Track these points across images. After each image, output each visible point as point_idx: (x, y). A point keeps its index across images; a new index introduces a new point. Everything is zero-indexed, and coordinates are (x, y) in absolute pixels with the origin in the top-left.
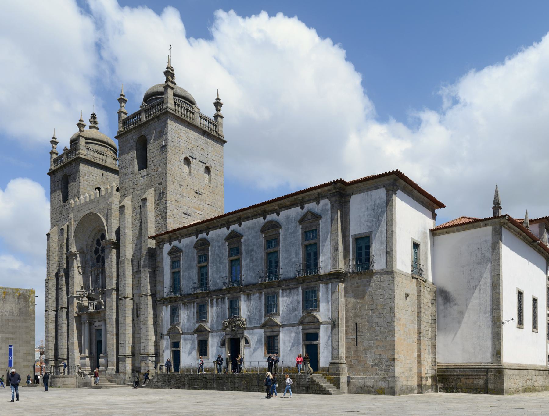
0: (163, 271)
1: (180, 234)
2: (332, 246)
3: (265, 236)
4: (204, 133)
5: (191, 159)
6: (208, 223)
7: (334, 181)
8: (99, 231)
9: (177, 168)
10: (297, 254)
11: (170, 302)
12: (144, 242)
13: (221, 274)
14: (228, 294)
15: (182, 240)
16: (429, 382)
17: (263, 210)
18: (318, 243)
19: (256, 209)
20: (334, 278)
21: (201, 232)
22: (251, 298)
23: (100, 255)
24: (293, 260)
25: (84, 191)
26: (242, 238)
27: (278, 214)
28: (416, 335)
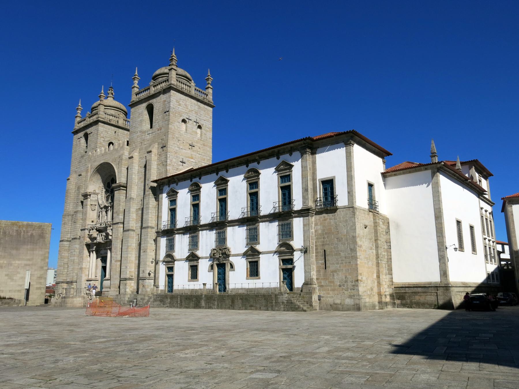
1: (178, 179)
2: (303, 188)
4: (198, 100)
5: (187, 120)
6: (201, 170)
7: (303, 138)
9: (176, 128)
11: (167, 234)
12: (148, 185)
14: (216, 226)
15: (179, 183)
16: (388, 299)
17: (246, 160)
19: (241, 159)
21: (195, 177)
26: (228, 182)
28: (375, 260)
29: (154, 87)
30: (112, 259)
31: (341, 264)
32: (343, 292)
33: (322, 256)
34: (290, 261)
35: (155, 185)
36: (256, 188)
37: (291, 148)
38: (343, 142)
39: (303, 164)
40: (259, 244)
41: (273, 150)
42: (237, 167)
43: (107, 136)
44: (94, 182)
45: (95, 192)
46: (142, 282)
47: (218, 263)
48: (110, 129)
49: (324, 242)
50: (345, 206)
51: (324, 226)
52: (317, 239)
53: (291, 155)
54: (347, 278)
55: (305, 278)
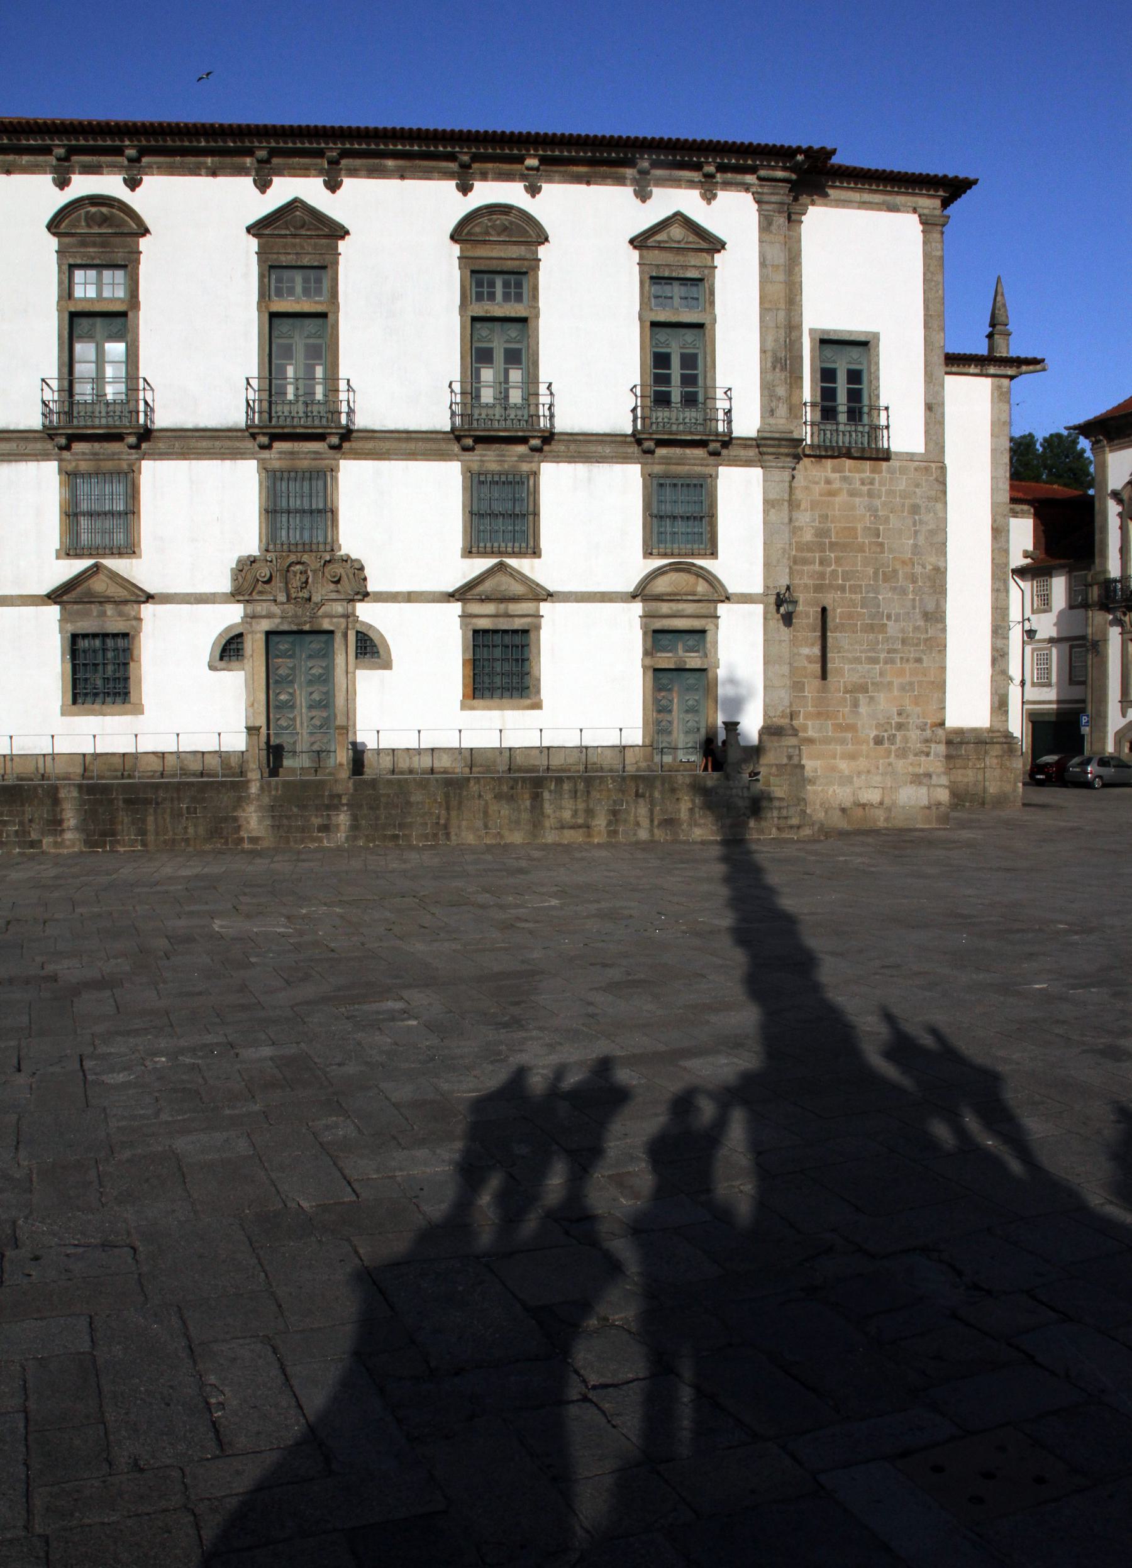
2: (763, 351)
3: (469, 254)
20: (777, 456)
26: (342, 238)
27: (533, 190)
31: (886, 663)
32: (890, 764)
36: (507, 297)
38: (915, 211)
39: (769, 257)
40: (536, 553)
42: (402, 177)
49: (824, 579)
50: (913, 454)
51: (824, 518)
52: (795, 562)
53: (709, 197)
54: (904, 715)
55: (766, 714)
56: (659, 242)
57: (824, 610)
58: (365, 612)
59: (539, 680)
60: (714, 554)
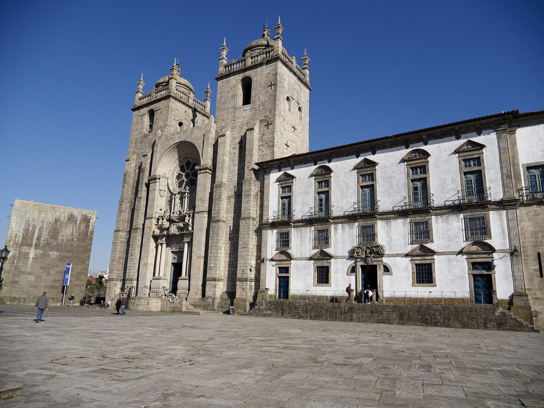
0: (268, 196)
1: (294, 161)
2: (502, 174)
4: (299, 79)
5: (291, 99)
8: (185, 158)
9: (282, 105)
10: (453, 181)
13: (349, 199)
18: (482, 170)
21: (321, 160)
22: (392, 224)
23: (183, 181)
24: (449, 187)
25: (171, 124)
26: (376, 165)
29: (252, 58)
30: (193, 255)
33: (536, 260)
34: (489, 266)
35: (256, 167)
37: (481, 124)
40: (432, 241)
41: (452, 127)
43: (177, 114)
44: (164, 164)
45: (165, 175)
46: (240, 284)
47: (365, 264)
48: (181, 108)
49: (537, 243)
56: (464, 149)
57: (539, 254)
58: (385, 260)
59: (435, 278)
60: (490, 237)
